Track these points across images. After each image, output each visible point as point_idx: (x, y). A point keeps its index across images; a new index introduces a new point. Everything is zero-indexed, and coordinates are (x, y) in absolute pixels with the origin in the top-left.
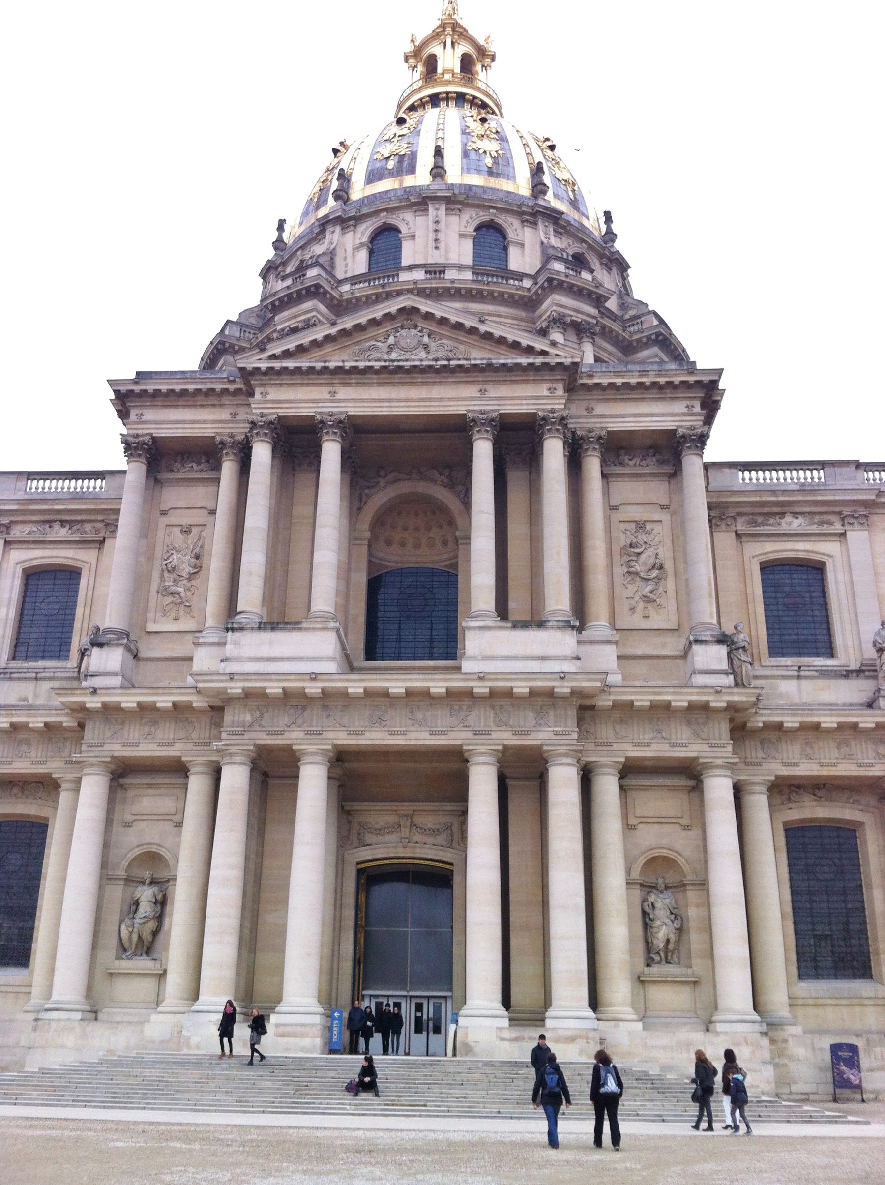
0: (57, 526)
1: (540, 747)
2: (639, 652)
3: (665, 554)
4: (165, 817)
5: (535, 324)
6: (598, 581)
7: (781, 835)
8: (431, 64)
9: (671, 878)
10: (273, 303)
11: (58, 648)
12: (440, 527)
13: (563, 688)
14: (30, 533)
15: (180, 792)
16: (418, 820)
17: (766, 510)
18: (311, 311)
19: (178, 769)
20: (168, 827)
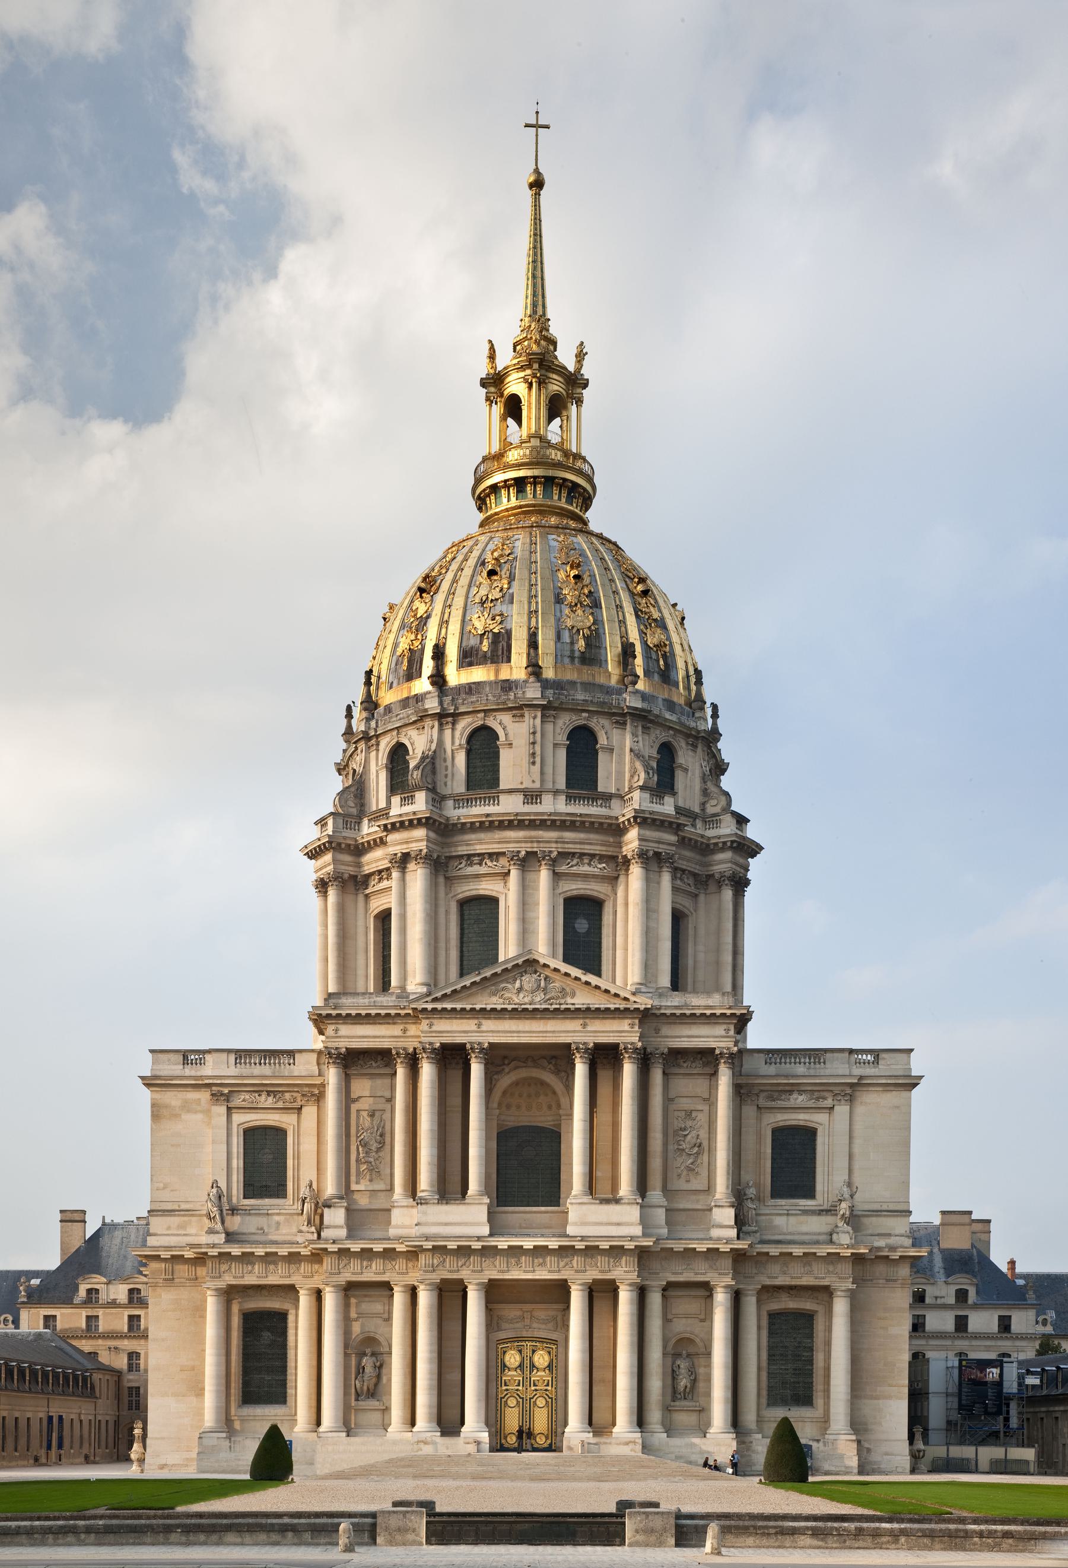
0: (264, 1096)
1: (614, 1281)
2: (681, 1206)
3: (703, 1134)
4: (377, 1315)
5: (621, 847)
6: (655, 1163)
7: (765, 1322)
8: (513, 408)
9: (691, 1350)
10: (385, 826)
11: (279, 1191)
12: (546, 1095)
13: (630, 1245)
14: (244, 1100)
15: (386, 1300)
16: (535, 1314)
17: (781, 1088)
18: (422, 840)
19: (387, 1287)
20: (379, 1321)
